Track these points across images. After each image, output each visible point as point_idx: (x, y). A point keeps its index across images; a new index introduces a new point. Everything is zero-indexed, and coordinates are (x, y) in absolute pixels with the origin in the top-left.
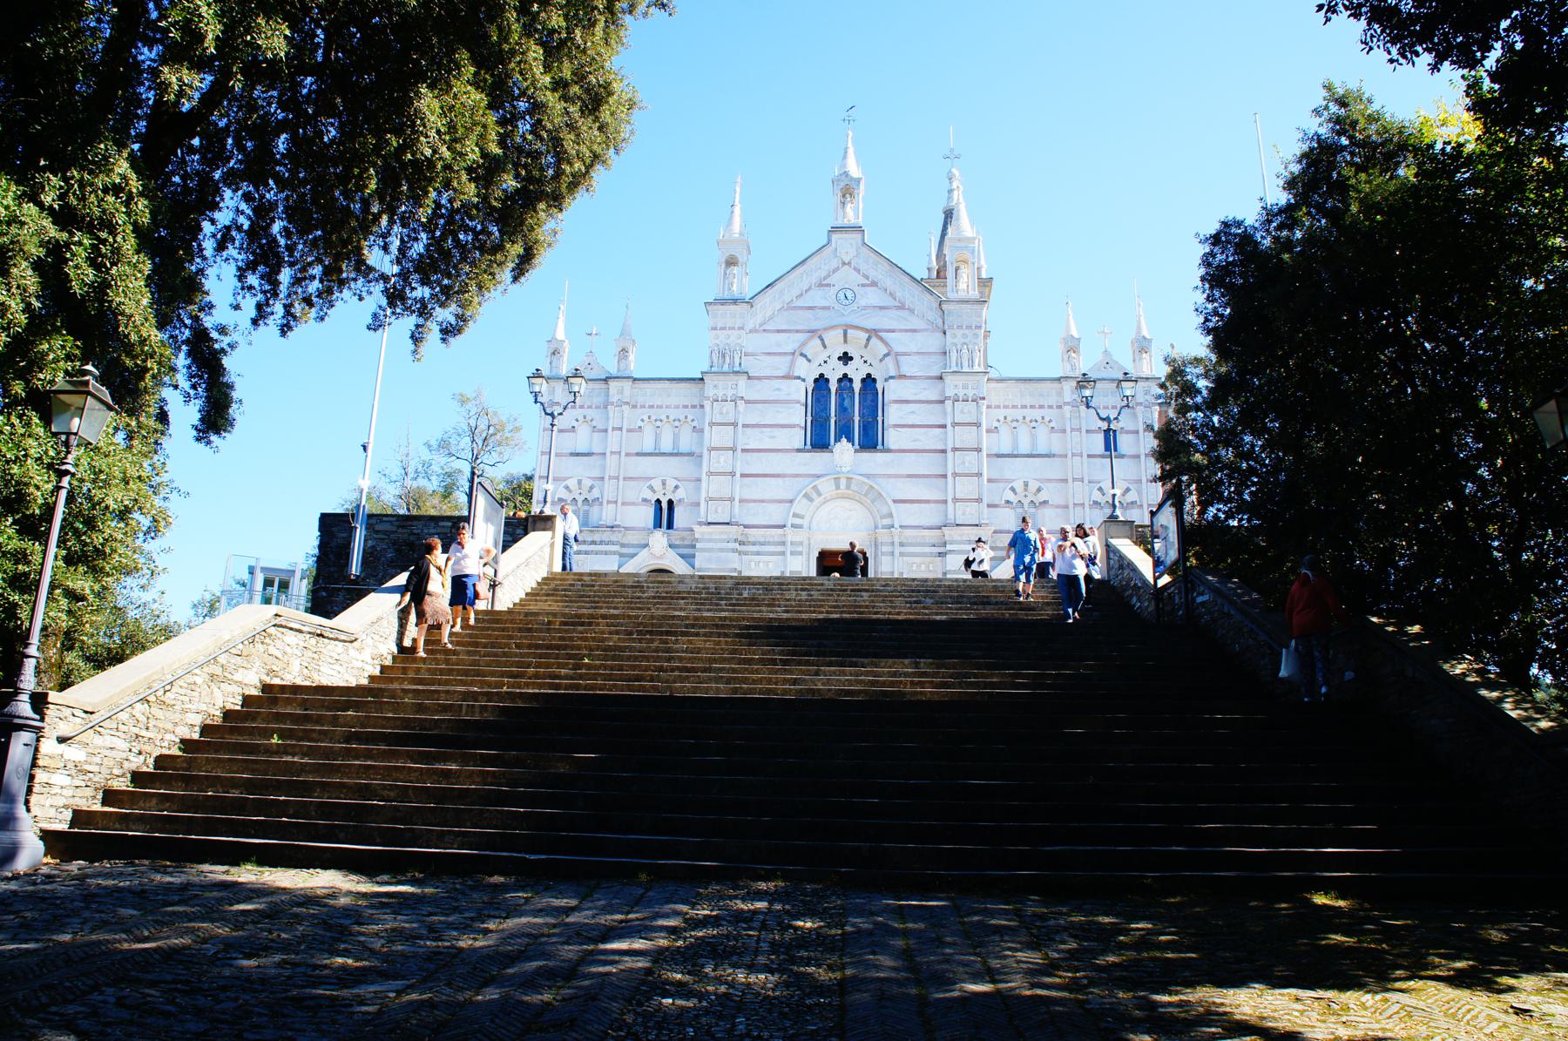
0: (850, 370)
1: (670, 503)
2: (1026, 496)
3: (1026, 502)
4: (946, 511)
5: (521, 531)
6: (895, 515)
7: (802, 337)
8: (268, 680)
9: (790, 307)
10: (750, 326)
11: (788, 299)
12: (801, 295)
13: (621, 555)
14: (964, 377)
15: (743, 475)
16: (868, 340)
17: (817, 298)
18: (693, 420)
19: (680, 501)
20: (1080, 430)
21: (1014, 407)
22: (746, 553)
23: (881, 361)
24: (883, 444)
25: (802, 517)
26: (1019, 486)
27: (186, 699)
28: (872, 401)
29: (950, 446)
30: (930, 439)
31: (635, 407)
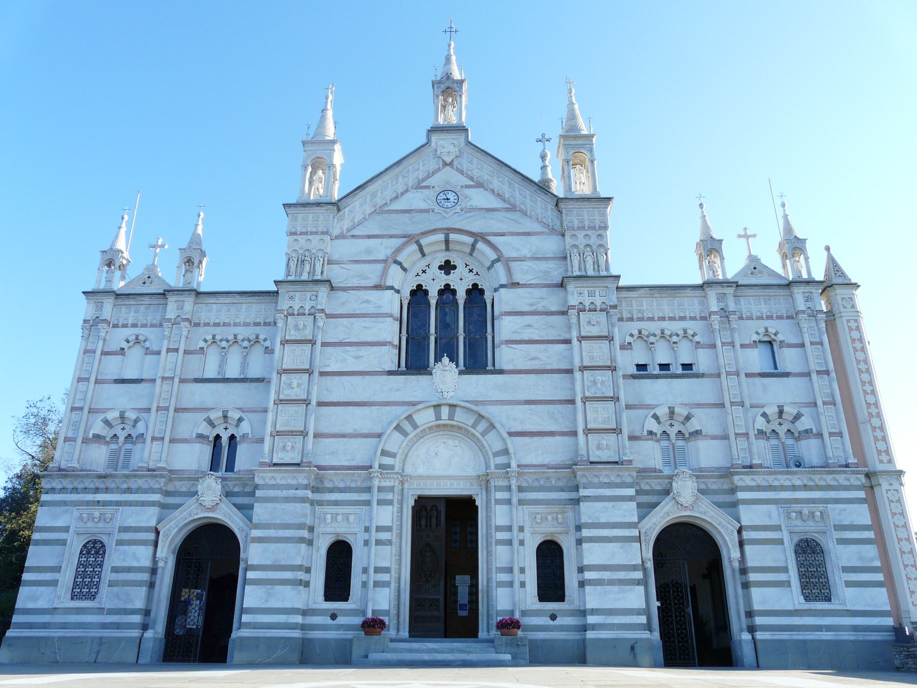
1: (232, 437)
2: (672, 425)
3: (673, 432)
4: (577, 444)
6: (511, 450)
7: (398, 242)
9: (381, 211)
10: (336, 232)
11: (379, 202)
12: (397, 198)
13: (163, 506)
14: (590, 283)
15: (320, 404)
16: (473, 246)
17: (416, 200)
18: (265, 340)
20: (732, 344)
22: (320, 503)
24: (494, 365)
25: (393, 455)
26: (662, 412)
29: (577, 363)
30: (552, 356)
31: (197, 325)
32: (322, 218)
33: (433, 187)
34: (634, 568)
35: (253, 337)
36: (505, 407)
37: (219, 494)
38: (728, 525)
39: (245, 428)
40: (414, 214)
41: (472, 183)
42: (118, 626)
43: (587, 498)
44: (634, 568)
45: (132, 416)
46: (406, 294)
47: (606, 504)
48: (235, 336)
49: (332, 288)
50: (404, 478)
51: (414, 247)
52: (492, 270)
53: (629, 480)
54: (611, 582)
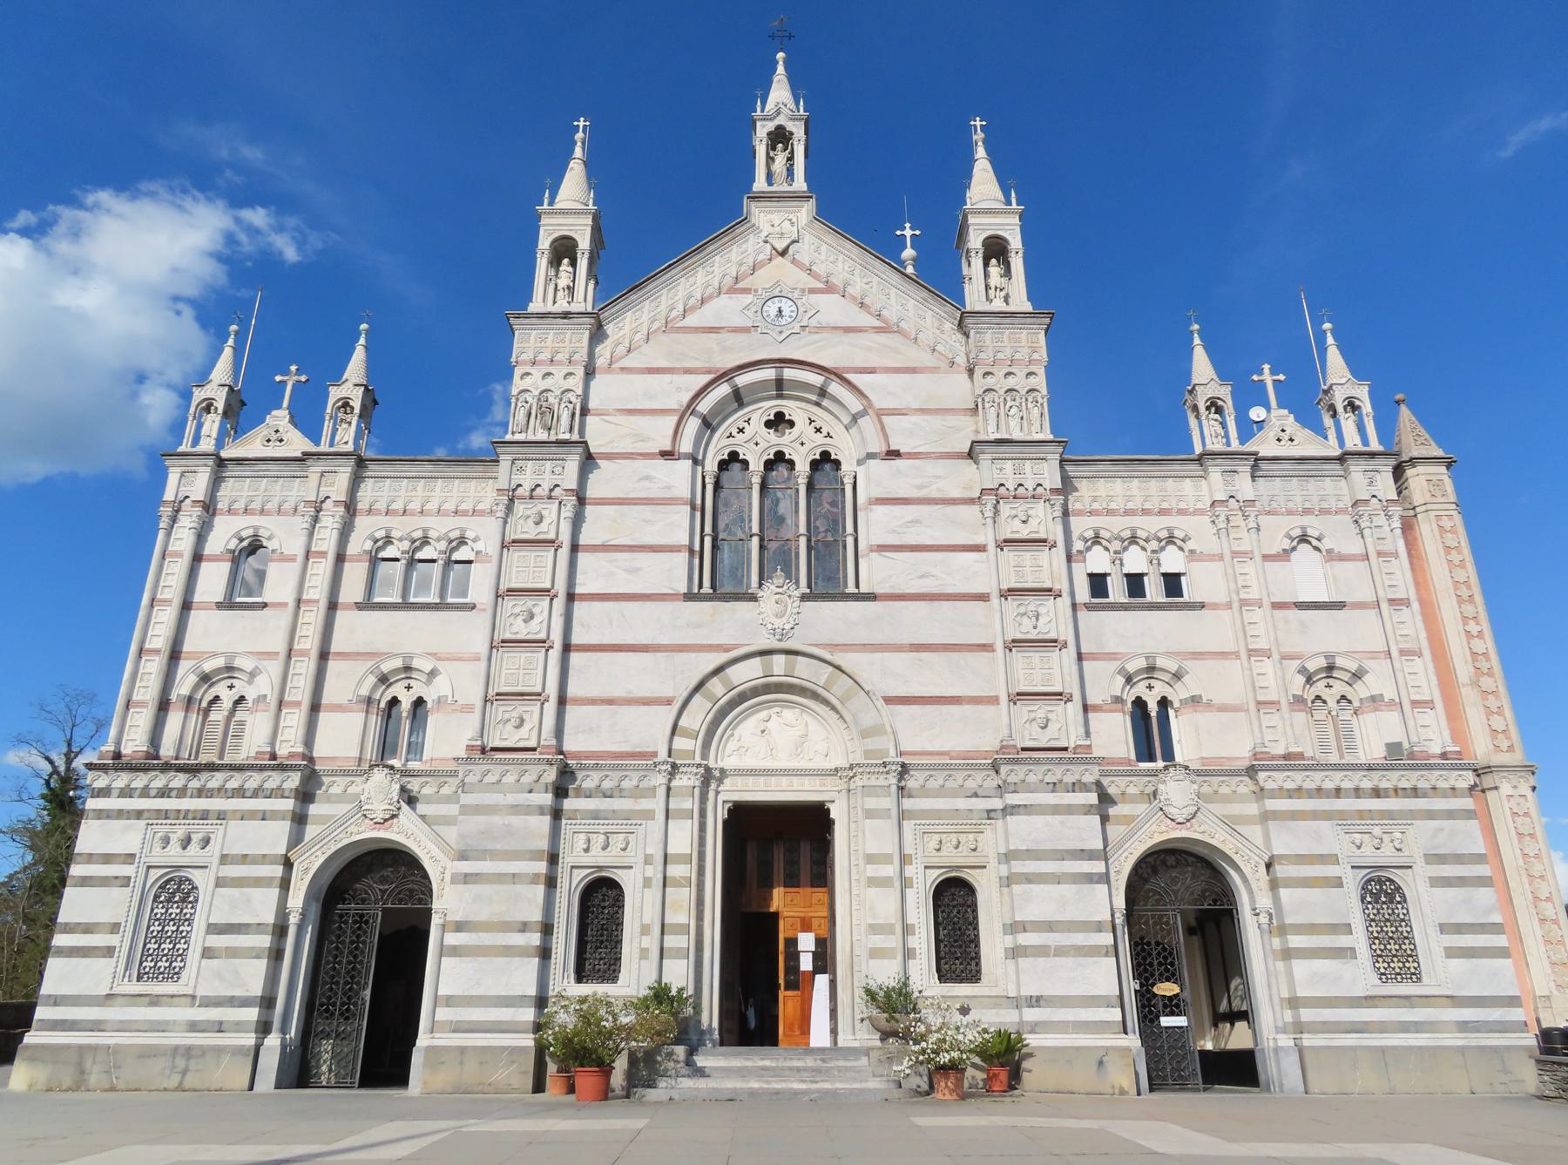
0: (784, 441)
1: (419, 703)
17: (728, 309)
18: (474, 540)
19: (440, 701)
24: (857, 586)
28: (833, 504)
33: (756, 291)
34: (1098, 927)
36: (879, 655)
37: (396, 799)
38: (1251, 854)
40: (724, 335)
41: (821, 286)
42: (220, 1027)
44: (1098, 927)
46: (711, 466)
47: (1049, 818)
52: (854, 430)
54: (1060, 952)
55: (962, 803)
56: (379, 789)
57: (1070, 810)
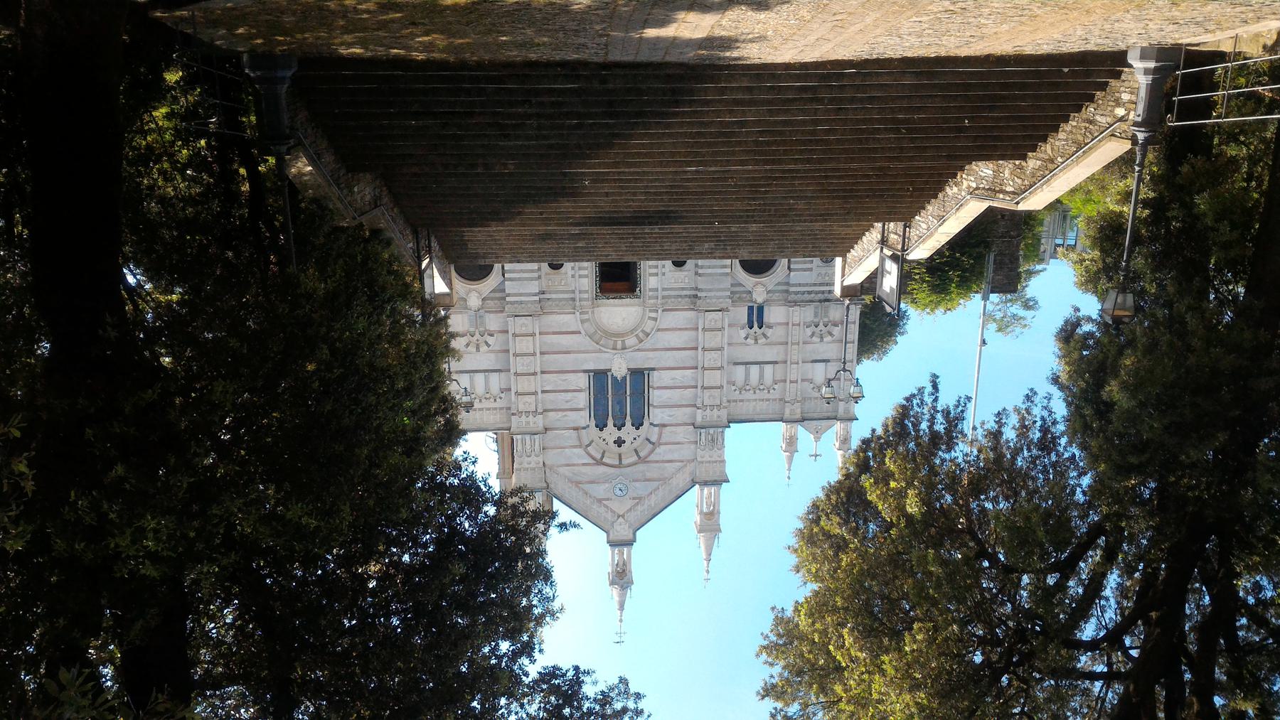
0: (616, 434)
1: (751, 327)
2: (478, 340)
5: (865, 285)
8: (1024, 164)
12: (655, 490)
14: (528, 430)
16: (603, 457)
17: (640, 488)
18: (735, 390)
21: (489, 409)
22: (692, 289)
23: (592, 441)
25: (650, 318)
26: (484, 348)
27: (1066, 147)
32: (702, 474)
35: (743, 392)
39: (743, 333)
43: (535, 295)
45: (815, 339)
46: (646, 423)
48: (755, 393)
49: (693, 424)
50: (644, 305)
51: (642, 454)
53: (509, 306)
55: (554, 296)
56: (759, 296)
57: (515, 295)
